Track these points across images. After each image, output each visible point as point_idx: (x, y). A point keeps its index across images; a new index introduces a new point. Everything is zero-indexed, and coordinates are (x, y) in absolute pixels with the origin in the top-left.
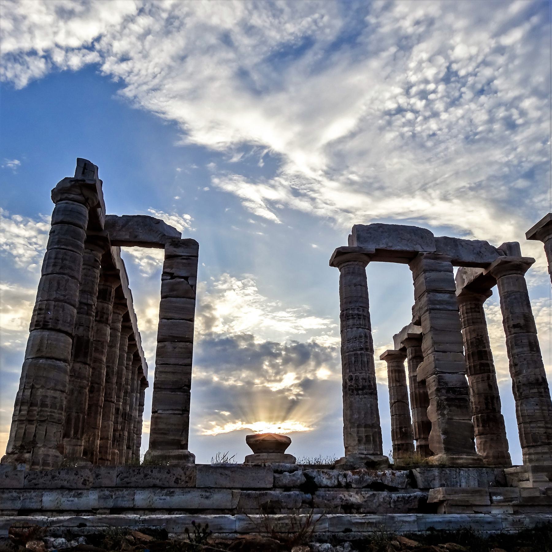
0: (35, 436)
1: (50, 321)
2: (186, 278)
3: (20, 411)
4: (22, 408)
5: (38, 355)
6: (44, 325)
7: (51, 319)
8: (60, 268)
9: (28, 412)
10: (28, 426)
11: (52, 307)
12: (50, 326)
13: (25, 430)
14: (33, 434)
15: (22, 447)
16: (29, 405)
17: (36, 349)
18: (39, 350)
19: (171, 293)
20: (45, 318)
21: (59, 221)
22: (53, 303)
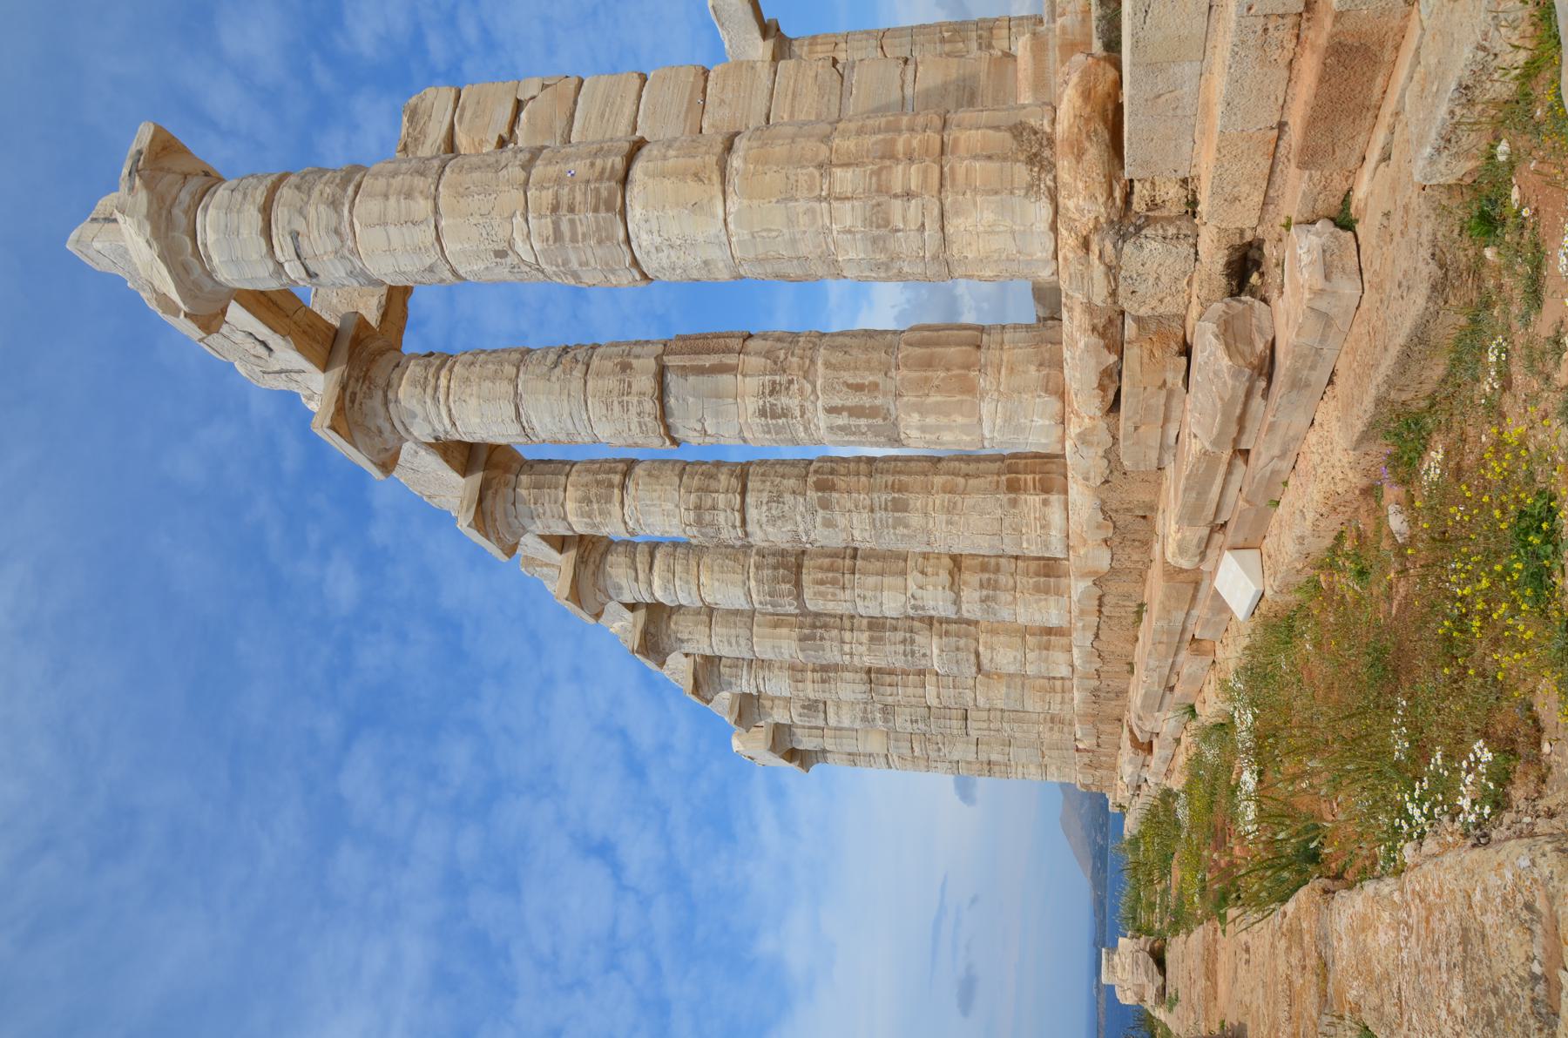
0: (997, 128)
1: (599, 162)
2: (519, 105)
3: (908, 195)
4: (899, 191)
5: (716, 178)
6: (609, 179)
7: (592, 164)
8: (422, 174)
9: (911, 159)
10: (962, 151)
11: (553, 170)
12: (619, 162)
13: (975, 157)
14: (991, 132)
15: (1032, 160)
16: (888, 163)
17: (692, 189)
18: (697, 177)
19: (559, 133)
20: (588, 182)
21: (256, 220)
22: (538, 170)
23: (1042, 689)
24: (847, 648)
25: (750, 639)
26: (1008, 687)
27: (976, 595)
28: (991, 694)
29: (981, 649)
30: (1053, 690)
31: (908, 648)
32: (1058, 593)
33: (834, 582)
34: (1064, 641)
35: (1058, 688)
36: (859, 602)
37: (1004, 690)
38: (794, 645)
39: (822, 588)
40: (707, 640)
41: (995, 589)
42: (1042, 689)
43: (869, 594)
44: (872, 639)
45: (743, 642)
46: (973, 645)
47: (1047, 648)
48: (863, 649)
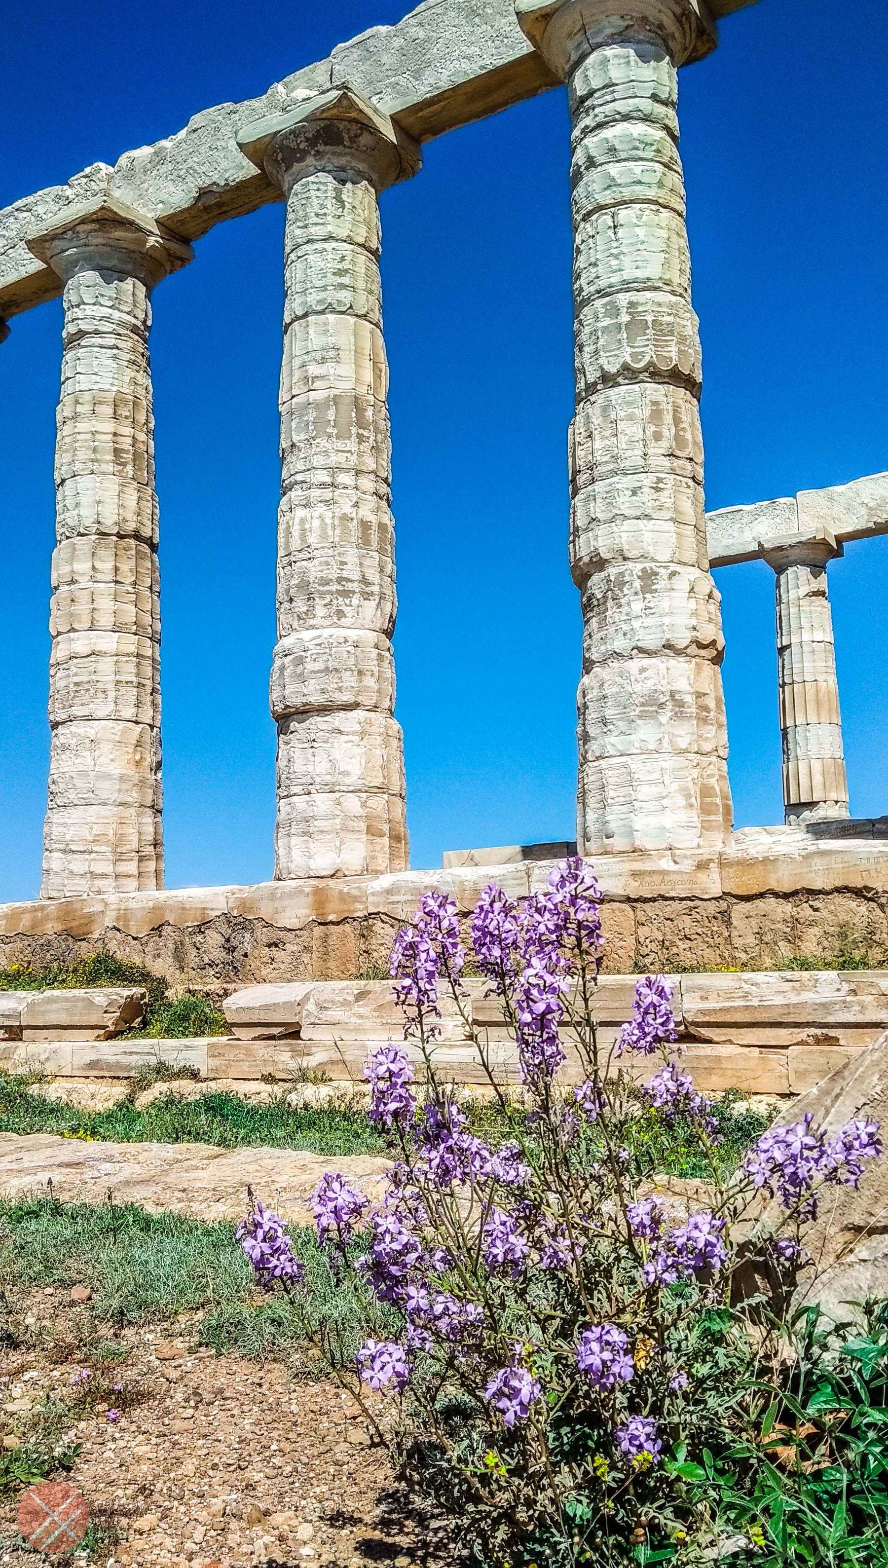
23: (121, 838)
24: (345, 478)
25: (349, 311)
26: (122, 778)
27: (682, 685)
28: (105, 747)
29: (359, 714)
30: (119, 858)
31: (355, 587)
32: (706, 827)
33: (679, 439)
34: (382, 862)
35: (123, 868)
36: (648, 480)
37: (116, 769)
38: (347, 386)
39: (668, 418)
40: (344, 233)
41: (698, 718)
42: (121, 838)
43: (665, 497)
44: (365, 525)
45: (345, 296)
46: (369, 700)
47: (369, 831)
48: (347, 509)
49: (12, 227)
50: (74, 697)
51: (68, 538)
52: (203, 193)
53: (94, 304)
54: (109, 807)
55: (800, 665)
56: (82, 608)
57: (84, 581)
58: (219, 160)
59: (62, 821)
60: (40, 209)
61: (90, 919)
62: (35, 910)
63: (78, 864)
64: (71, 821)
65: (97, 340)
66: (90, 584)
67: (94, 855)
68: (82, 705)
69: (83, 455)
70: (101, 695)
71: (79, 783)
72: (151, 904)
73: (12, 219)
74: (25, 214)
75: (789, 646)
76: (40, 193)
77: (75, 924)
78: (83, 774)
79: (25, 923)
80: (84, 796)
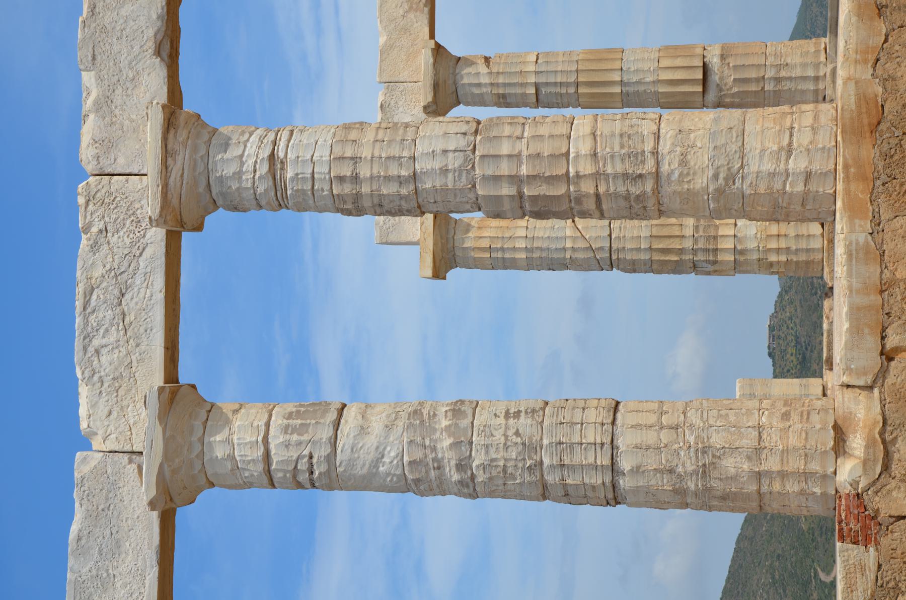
49: (101, 315)
50: (634, 148)
51: (473, 167)
52: (158, 52)
53: (245, 146)
54: (747, 118)
55: (559, 75)
56: (546, 149)
57: (522, 146)
58: (135, 27)
59: (757, 158)
60: (98, 272)
61: (863, 99)
62: (847, 179)
63: (802, 138)
64: (759, 146)
65: (282, 145)
66: (525, 141)
67: (794, 125)
68: (643, 142)
69: (395, 151)
70: (635, 128)
71: (721, 141)
72: (854, 19)
73: (92, 318)
74: (94, 297)
75: (537, 86)
76: (78, 273)
77: (865, 121)
78: (714, 135)
79: (861, 192)
80: (735, 135)
